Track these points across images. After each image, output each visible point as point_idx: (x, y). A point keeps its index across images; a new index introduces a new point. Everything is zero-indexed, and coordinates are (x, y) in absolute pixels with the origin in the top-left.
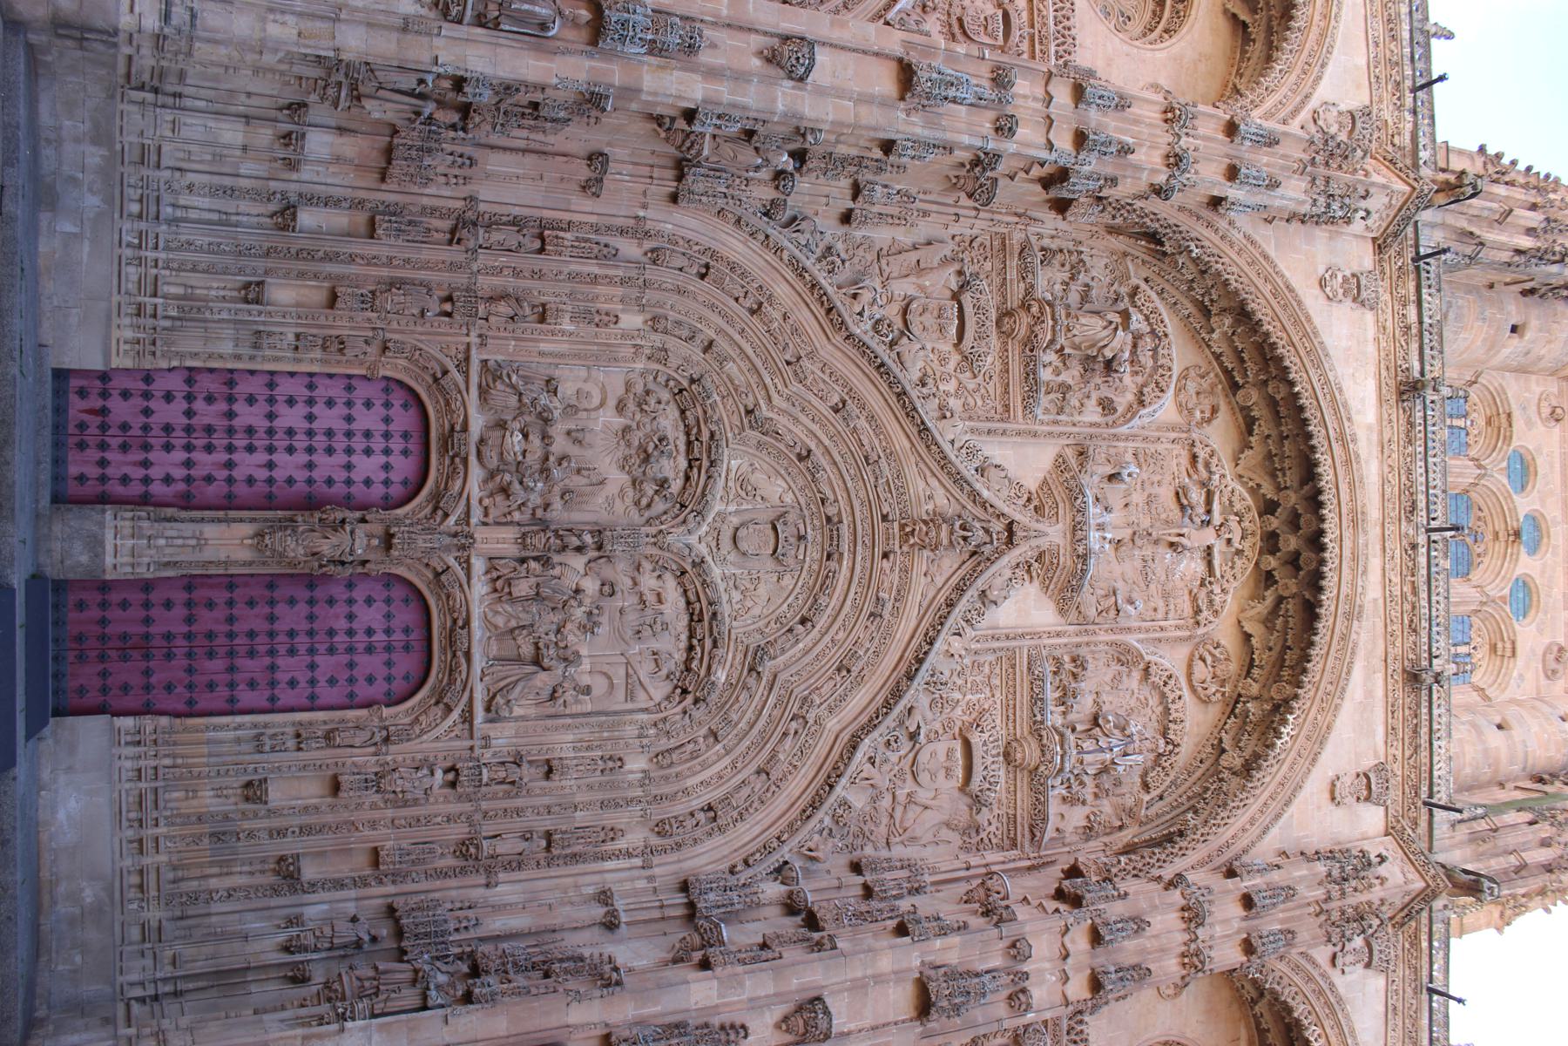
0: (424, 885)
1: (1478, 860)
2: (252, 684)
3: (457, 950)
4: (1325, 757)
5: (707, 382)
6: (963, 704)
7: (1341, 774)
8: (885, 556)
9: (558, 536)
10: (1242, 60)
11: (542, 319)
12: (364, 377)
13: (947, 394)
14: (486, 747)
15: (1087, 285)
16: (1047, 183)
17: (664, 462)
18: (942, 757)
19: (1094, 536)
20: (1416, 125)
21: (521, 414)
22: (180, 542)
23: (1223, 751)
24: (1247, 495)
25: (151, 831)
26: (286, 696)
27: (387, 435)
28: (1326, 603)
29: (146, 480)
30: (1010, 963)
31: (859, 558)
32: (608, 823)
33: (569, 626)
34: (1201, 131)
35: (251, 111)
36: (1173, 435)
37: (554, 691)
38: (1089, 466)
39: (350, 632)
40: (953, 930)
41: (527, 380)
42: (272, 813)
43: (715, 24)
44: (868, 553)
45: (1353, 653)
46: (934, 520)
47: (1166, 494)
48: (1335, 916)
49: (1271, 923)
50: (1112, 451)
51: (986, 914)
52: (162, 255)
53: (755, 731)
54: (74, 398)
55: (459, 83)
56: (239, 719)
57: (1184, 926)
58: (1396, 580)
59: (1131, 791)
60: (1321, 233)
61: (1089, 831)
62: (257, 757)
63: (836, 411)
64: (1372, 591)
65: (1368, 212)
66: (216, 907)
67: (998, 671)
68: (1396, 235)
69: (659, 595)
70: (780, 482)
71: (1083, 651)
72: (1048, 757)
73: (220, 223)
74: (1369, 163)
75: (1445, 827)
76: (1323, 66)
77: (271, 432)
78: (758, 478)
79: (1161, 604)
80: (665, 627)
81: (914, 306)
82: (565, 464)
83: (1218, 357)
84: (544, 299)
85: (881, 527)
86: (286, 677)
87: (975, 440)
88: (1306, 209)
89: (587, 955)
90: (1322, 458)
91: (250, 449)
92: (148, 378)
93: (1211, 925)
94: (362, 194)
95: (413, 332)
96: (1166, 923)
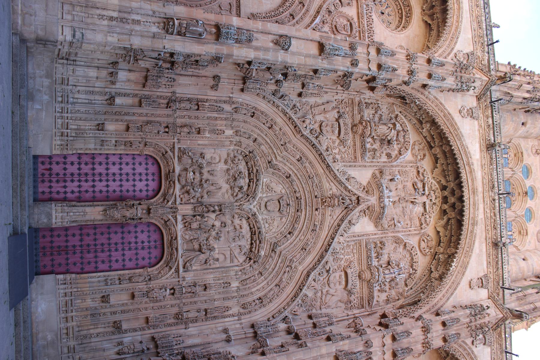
0: (164, 329)
1: (520, 306)
2: (103, 262)
3: (177, 352)
5: (255, 153)
6: (344, 259)
7: (473, 278)
8: (316, 210)
9: (206, 207)
10: (429, 36)
11: (199, 133)
12: (139, 155)
13: (335, 154)
14: (184, 281)
15: (381, 115)
16: (368, 81)
17: (241, 180)
18: (338, 278)
19: (386, 200)
20: (489, 57)
21: (192, 165)
22: (78, 214)
23: (432, 272)
24: (436, 184)
25: (70, 314)
26: (115, 266)
27: (147, 174)
28: (465, 220)
29: (65, 193)
30: (366, 349)
31: (308, 211)
32: (226, 305)
33: (211, 238)
34: (419, 62)
35: (99, 65)
36: (411, 165)
37: (206, 260)
38: (384, 176)
39: (136, 243)
40: (346, 338)
41: (194, 154)
42: (111, 306)
43: (257, 32)
44: (311, 209)
45: (475, 237)
46: (332, 197)
47: (409, 185)
48: (473, 328)
49: (452, 331)
50: (391, 171)
51: (356, 332)
52: (70, 115)
53: (274, 272)
54: (40, 165)
55: (172, 55)
56: (99, 274)
57: (423, 333)
58: (489, 211)
59: (401, 287)
60: (459, 95)
61: (388, 301)
62: (106, 287)
63: (299, 161)
64: (481, 216)
65: (475, 87)
66: (93, 340)
68: (484, 95)
69: (240, 226)
70: (280, 186)
71: (384, 240)
72: (374, 276)
73: (89, 103)
74: (474, 71)
75: (508, 295)
76: (457, 38)
77: (107, 174)
78: (273, 185)
79: (409, 222)
80: (243, 237)
81: (323, 124)
82: (208, 182)
83: (425, 137)
84: (199, 126)
85: (315, 200)
87: (346, 169)
89: (221, 351)
91: (101, 181)
92: (65, 157)
94: (137, 92)
95: (155, 139)
96: (417, 333)
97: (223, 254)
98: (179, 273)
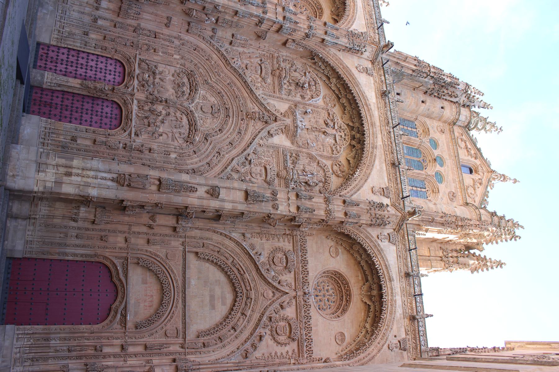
4: (369, 180)
8: (242, 120)
11: (155, 52)
16: (278, 31)
18: (259, 171)
20: (379, 36)
27: (115, 72)
28: (366, 145)
30: (273, 196)
31: (234, 119)
33: (157, 120)
39: (102, 112)
45: (375, 157)
47: (321, 122)
48: (374, 215)
52: (66, 22)
64: (379, 143)
68: (376, 59)
78: (208, 96)
79: (321, 147)
83: (334, 91)
86: (84, 119)
87: (265, 97)
88: (348, 45)
90: (361, 109)
91: (82, 68)
92: (59, 48)
93: (334, 205)
94: (113, 19)
97: (166, 134)
98: (131, 136)
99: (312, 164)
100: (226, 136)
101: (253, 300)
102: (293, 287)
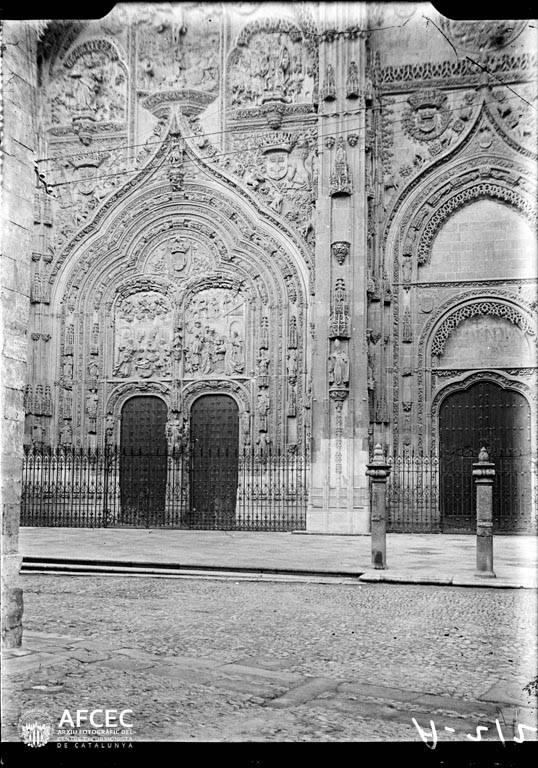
8: (187, 198)
67: (237, 136)
71: (231, 86)
79: (211, 39)
99: (247, 58)
100: (220, 225)
101: (494, 167)
102: (472, 91)
